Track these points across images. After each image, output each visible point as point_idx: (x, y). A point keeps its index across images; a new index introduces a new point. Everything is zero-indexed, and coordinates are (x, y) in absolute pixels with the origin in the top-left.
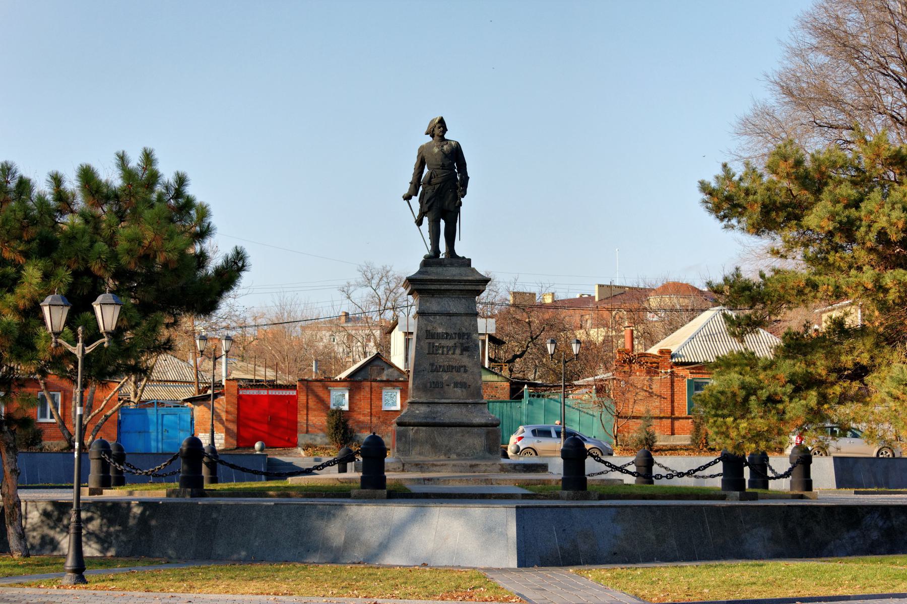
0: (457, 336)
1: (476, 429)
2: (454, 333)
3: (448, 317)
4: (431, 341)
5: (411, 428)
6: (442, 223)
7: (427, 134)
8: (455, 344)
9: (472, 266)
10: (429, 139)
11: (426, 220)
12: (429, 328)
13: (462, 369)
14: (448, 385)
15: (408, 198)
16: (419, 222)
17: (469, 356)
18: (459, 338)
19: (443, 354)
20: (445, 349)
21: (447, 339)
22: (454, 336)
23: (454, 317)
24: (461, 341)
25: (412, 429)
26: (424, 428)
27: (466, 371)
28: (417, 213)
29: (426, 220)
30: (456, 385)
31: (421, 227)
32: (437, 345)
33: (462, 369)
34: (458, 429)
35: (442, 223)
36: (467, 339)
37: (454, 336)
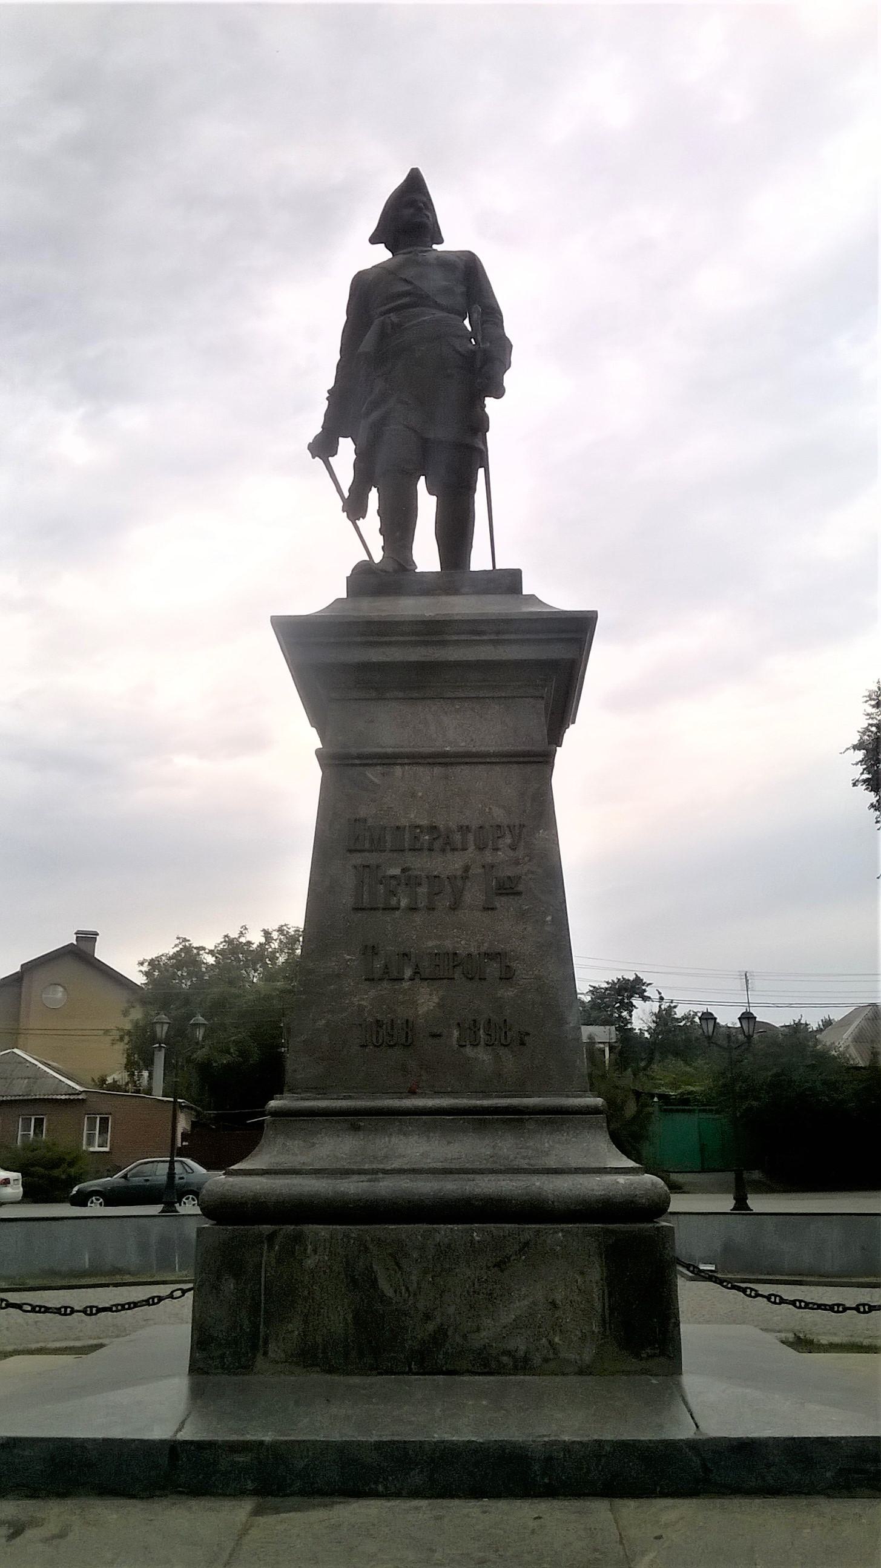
0: (471, 837)
1: (556, 1234)
2: (461, 828)
3: (437, 770)
4: (372, 859)
5: (267, 1229)
6: (427, 505)
7: (374, 240)
8: (467, 869)
9: (526, 591)
10: (381, 254)
11: (373, 496)
12: (362, 812)
13: (493, 969)
14: (434, 1036)
15: (324, 447)
16: (355, 508)
17: (522, 915)
18: (481, 849)
19: (413, 909)
20: (423, 890)
21: (431, 850)
22: (458, 837)
23: (458, 769)
24: (488, 857)
25: (271, 1237)
26: (323, 1231)
27: (507, 977)
28: (346, 478)
29: (373, 496)
30: (470, 1031)
31: (360, 523)
32: (396, 871)
33: (493, 969)
34: (477, 1232)
35: (427, 505)
36: (513, 848)
37: (458, 837)
